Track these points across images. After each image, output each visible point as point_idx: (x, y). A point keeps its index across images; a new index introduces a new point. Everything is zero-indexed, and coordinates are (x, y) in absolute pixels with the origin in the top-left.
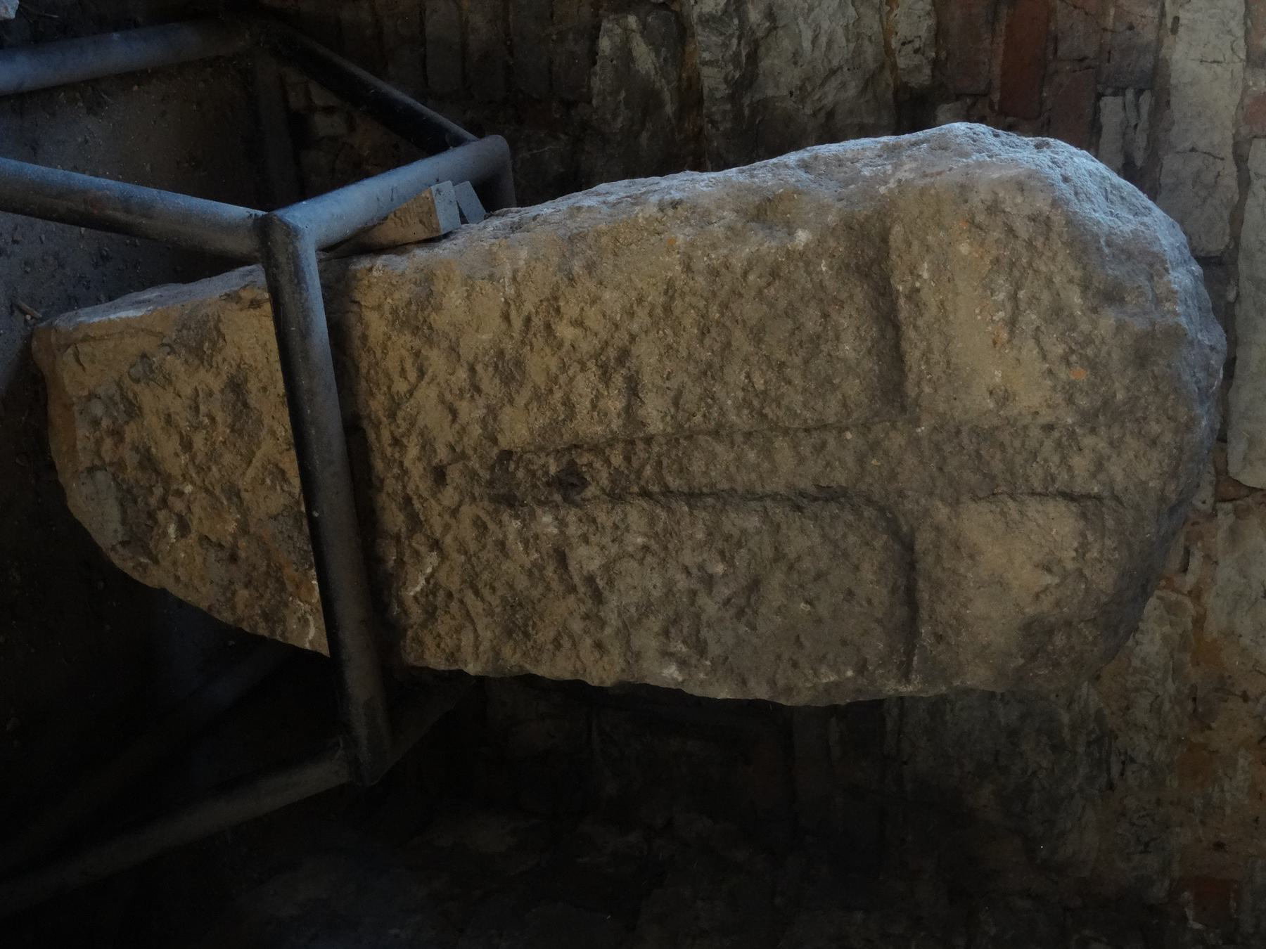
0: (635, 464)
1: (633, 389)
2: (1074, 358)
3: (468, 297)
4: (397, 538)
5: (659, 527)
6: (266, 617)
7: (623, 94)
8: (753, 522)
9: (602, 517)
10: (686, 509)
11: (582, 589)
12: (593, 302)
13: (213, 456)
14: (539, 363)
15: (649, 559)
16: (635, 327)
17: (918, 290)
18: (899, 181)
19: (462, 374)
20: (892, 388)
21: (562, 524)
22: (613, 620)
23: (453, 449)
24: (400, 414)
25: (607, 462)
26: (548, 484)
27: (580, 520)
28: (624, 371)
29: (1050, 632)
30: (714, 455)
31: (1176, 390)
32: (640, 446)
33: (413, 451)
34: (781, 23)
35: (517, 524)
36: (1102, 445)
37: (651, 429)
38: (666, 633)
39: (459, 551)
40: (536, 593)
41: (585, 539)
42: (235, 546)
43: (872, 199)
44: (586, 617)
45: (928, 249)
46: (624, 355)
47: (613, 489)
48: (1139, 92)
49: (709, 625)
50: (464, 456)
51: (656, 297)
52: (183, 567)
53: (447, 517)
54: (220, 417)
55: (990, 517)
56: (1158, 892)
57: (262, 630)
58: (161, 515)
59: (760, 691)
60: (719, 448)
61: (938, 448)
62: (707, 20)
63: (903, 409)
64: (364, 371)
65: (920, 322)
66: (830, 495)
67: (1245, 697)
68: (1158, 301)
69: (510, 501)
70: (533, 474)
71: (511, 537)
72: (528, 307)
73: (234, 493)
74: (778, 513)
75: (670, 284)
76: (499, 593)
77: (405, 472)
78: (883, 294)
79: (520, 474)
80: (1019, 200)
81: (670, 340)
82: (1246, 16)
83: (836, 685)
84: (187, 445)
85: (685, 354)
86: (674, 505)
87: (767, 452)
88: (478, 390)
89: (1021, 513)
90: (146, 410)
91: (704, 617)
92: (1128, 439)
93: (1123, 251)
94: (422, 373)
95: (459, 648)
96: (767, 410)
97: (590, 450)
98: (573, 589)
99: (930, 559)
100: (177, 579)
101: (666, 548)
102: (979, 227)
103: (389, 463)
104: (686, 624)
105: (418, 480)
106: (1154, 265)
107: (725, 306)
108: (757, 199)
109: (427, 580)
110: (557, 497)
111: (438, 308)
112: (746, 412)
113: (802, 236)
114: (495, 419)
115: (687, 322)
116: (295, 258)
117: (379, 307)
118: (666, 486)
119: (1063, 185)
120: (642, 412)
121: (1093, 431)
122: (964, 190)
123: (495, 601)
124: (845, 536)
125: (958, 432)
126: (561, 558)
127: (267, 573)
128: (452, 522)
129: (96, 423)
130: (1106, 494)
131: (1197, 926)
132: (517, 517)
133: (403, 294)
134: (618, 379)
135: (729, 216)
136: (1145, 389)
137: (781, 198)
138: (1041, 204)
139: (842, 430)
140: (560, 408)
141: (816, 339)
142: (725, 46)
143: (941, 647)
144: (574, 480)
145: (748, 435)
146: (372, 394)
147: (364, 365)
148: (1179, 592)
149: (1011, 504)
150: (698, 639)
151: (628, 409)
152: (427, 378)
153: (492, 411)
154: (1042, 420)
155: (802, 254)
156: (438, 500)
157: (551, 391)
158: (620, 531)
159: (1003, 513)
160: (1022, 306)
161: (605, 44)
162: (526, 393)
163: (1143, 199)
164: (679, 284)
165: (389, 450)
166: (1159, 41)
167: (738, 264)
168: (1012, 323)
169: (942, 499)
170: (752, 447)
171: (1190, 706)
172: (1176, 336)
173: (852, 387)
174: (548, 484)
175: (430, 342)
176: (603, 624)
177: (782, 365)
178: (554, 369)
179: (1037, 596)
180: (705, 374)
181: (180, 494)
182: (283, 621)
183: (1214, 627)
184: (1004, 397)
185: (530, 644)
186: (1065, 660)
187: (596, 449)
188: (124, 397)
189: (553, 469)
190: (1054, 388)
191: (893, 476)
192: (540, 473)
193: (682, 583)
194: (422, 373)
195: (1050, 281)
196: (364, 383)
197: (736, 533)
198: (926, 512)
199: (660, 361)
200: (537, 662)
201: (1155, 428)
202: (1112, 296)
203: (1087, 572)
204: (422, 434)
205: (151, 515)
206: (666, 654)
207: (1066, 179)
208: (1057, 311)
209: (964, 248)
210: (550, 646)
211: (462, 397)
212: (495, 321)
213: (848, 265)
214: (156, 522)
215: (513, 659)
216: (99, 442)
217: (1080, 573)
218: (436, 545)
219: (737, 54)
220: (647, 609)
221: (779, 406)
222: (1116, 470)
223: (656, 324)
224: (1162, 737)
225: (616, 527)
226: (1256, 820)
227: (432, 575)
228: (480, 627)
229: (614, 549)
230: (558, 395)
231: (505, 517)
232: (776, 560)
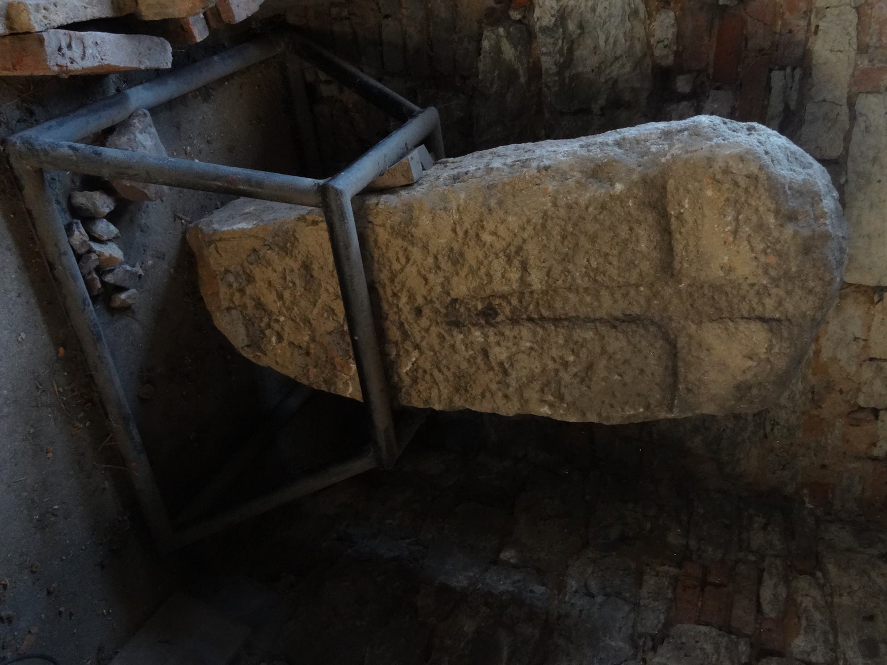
0: (525, 304)
1: (525, 267)
2: (769, 251)
3: (433, 220)
4: (396, 343)
5: (539, 338)
6: (325, 381)
7: (496, 73)
8: (589, 335)
9: (507, 332)
10: (553, 327)
11: (497, 369)
12: (502, 223)
13: (294, 303)
14: (473, 255)
15: (533, 353)
16: (526, 236)
17: (682, 213)
18: (673, 155)
19: (430, 260)
20: (667, 267)
21: (486, 336)
22: (514, 384)
23: (425, 298)
24: (396, 280)
25: (509, 303)
27: (496, 334)
28: (519, 258)
29: (750, 388)
31: (824, 265)
33: (404, 299)
34: (587, 30)
35: (461, 336)
36: (782, 293)
37: (534, 288)
38: (542, 391)
39: (430, 350)
41: (498, 344)
42: (308, 347)
43: (657, 165)
44: (499, 383)
45: (688, 192)
46: (519, 250)
47: (512, 317)
48: (794, 69)
49: (565, 386)
50: (431, 302)
51: (537, 220)
52: (280, 357)
53: (423, 333)
54: (298, 282)
55: (719, 331)
56: (790, 489)
57: (324, 388)
58: (268, 332)
59: (592, 418)
60: (571, 296)
61: (691, 295)
62: (545, 30)
63: (672, 275)
64: (376, 258)
65: (683, 230)
66: (630, 319)
67: (841, 392)
68: (816, 218)
69: (456, 324)
70: (469, 310)
71: (458, 343)
72: (467, 225)
73: (307, 321)
74: (603, 329)
75: (545, 213)
76: (452, 370)
77: (400, 310)
78: (664, 215)
79: (462, 310)
80: (741, 166)
82: (858, 24)
83: (634, 415)
84: (281, 297)
85: (553, 249)
86: (546, 325)
87: (597, 296)
88: (439, 268)
89: (736, 328)
90: (257, 278)
91: (563, 383)
92: (797, 289)
93: (798, 192)
95: (430, 397)
96: (598, 278)
97: (500, 297)
98: (492, 369)
99: (685, 351)
100: (277, 363)
102: (718, 181)
103: (391, 305)
106: (815, 197)
107: (575, 225)
109: (413, 364)
110: (483, 322)
111: (416, 226)
112: (586, 279)
114: (449, 282)
115: (555, 233)
116: (341, 207)
118: (541, 315)
119: (765, 157)
120: (529, 279)
121: (777, 286)
122: (710, 161)
123: (449, 374)
125: (702, 287)
126: (485, 353)
127: (327, 361)
128: (426, 335)
129: (230, 285)
130: (783, 318)
131: (811, 506)
132: (461, 333)
133: (397, 219)
134: (516, 263)
135: (578, 175)
136: (807, 266)
137: (606, 164)
138: (754, 169)
140: (485, 278)
141: (626, 242)
142: (555, 44)
143: (690, 395)
144: (490, 312)
145: (586, 289)
146: (381, 271)
147: (376, 256)
149: (731, 324)
151: (522, 278)
152: (411, 262)
153: (447, 279)
154: (748, 281)
155: (618, 197)
157: (479, 269)
158: (517, 340)
159: (726, 329)
160: (741, 223)
161: (486, 44)
164: (549, 213)
165: (390, 299)
166: (807, 39)
167: (583, 202)
168: (735, 233)
169: (692, 322)
170: (588, 295)
171: (810, 396)
172: (826, 237)
173: (645, 266)
174: (477, 315)
175: (413, 244)
176: (508, 386)
177: (607, 254)
178: (481, 257)
179: (744, 372)
180: (564, 260)
181: (277, 321)
182: (335, 384)
183: (825, 356)
184: (730, 270)
185: (468, 395)
186: (756, 400)
187: (503, 297)
188: (244, 272)
189: (480, 307)
190: (757, 266)
191: (666, 309)
192: (472, 309)
193: (551, 365)
196: (376, 265)
197: (581, 340)
198: (684, 328)
199: (539, 253)
200: (473, 405)
201: (811, 284)
202: (792, 217)
203: (772, 359)
204: (409, 291)
205: (262, 332)
206: (543, 401)
207: (766, 153)
208: (761, 226)
211: (430, 272)
212: (449, 233)
213: (644, 203)
214: (264, 334)
215: (459, 403)
216: (232, 295)
217: (768, 360)
218: (417, 347)
219: (562, 49)
220: (531, 379)
221: (604, 275)
222: (789, 306)
223: (537, 234)
224: (794, 412)
225: (515, 337)
226: (845, 453)
227: (415, 362)
229: (514, 349)
230: (483, 270)
231: (455, 333)
232: (602, 354)
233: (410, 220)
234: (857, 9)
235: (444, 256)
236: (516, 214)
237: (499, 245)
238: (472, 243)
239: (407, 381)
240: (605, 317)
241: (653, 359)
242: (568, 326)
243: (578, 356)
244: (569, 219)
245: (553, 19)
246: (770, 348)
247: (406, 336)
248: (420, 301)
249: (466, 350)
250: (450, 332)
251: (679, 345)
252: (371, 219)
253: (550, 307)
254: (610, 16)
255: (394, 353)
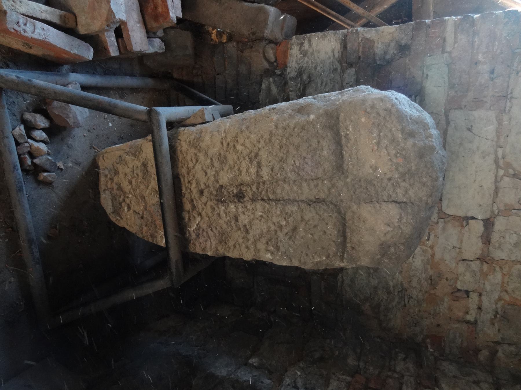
1: (259, 165)
2: (398, 155)
4: (189, 212)
5: (266, 210)
6: (151, 236)
7: (268, 100)
8: (295, 208)
11: (242, 229)
12: (248, 138)
13: (138, 186)
14: (231, 157)
15: (263, 219)
16: (260, 146)
17: (348, 135)
18: (343, 100)
19: (209, 161)
20: (340, 167)
21: (237, 208)
22: (252, 239)
24: (191, 174)
25: (251, 189)
26: (233, 196)
28: (257, 160)
29: (389, 247)
30: (284, 188)
31: (432, 167)
32: (261, 184)
33: (194, 185)
34: (312, 79)
35: (223, 208)
36: (407, 186)
37: (264, 179)
38: (267, 243)
40: (229, 230)
42: (143, 213)
43: (334, 105)
44: (243, 238)
45: (352, 121)
46: (257, 155)
47: (253, 198)
48: (416, 96)
50: (209, 187)
52: (129, 221)
53: (203, 205)
54: (140, 174)
55: (370, 208)
56: (420, 338)
57: (150, 240)
58: (123, 204)
59: (296, 264)
60: (286, 186)
61: (354, 186)
62: (292, 79)
63: (343, 173)
64: (180, 160)
65: (349, 145)
66: (318, 201)
67: (447, 279)
68: (427, 138)
71: (222, 212)
73: (143, 198)
74: (303, 205)
75: (271, 132)
76: (218, 230)
77: (191, 191)
78: (337, 134)
81: (271, 150)
82: (448, 73)
83: (320, 262)
84: (130, 183)
85: (275, 154)
86: (271, 203)
87: (300, 187)
88: (214, 166)
89: (380, 207)
90: (120, 172)
91: (279, 239)
92: (416, 183)
93: (415, 121)
94: (197, 161)
95: (206, 247)
96: (300, 173)
98: (240, 229)
99: (350, 222)
100: (127, 224)
101: (268, 216)
102: (368, 113)
103: (187, 188)
104: (274, 240)
105: (195, 194)
106: (425, 126)
107: (287, 139)
108: (299, 107)
109: (197, 225)
110: (236, 200)
111: (202, 141)
112: (293, 173)
113: (312, 117)
114: (218, 175)
115: (276, 144)
116: (158, 121)
117: (185, 141)
120: (261, 173)
121: (404, 181)
122: (364, 101)
124: (323, 213)
125: (360, 181)
127: (152, 222)
128: (204, 207)
129: (106, 176)
130: (408, 201)
131: (431, 350)
132: (223, 206)
133: (193, 137)
134: (255, 163)
135: (290, 111)
136: (422, 166)
138: (389, 106)
139: (323, 180)
140: (237, 171)
141: (315, 150)
142: (296, 86)
143: (354, 251)
144: (241, 195)
145: (294, 181)
146: (182, 167)
147: (180, 158)
148: (426, 246)
149: (377, 204)
150: (277, 246)
151: (257, 172)
152: (198, 162)
153: (217, 173)
154: (387, 176)
155: (312, 122)
156: (201, 200)
157: (235, 166)
158: (254, 210)
159: (374, 207)
160: (382, 138)
161: (263, 86)
162: (227, 166)
163: (420, 108)
164: (273, 132)
165: (187, 185)
166: (422, 82)
168: (378, 143)
169: (354, 202)
170: (295, 185)
171: (430, 281)
172: (432, 149)
173: (327, 165)
174: (233, 196)
175: (200, 151)
176: (248, 240)
177: (305, 158)
178: (236, 159)
180: (281, 161)
181: (128, 197)
182: (156, 237)
183: (437, 257)
185: (227, 246)
186: (393, 257)
187: (248, 185)
188: (114, 168)
189: (235, 192)
190: (392, 165)
192: (231, 193)
193: (273, 228)
194: (197, 161)
195: (391, 130)
196: (180, 164)
197: (290, 212)
198: (350, 207)
200: (229, 252)
201: (425, 179)
202: (411, 135)
203: (402, 227)
204: (196, 180)
205: (120, 204)
206: (267, 250)
207: (396, 99)
208: (393, 140)
209: (363, 120)
210: (233, 247)
211: (208, 168)
212: (219, 144)
213: (326, 126)
214: (122, 206)
215: (222, 251)
216: (107, 182)
217: (400, 228)
218: (200, 214)
219: (300, 88)
220: (261, 236)
221: (304, 171)
222: (411, 193)
223: (266, 145)
224: (421, 291)
225: (253, 209)
226: (450, 318)
227: (198, 224)
228: (212, 240)
229: (252, 216)
230: (237, 167)
231: (220, 206)
232: (302, 221)
233: (199, 139)
237: (245, 152)
238: (231, 151)
239: (194, 236)
240: (304, 199)
242: (283, 204)
246: (400, 219)
247: (194, 207)
250: (217, 205)
251: (347, 218)
252: (180, 138)
253: (274, 192)
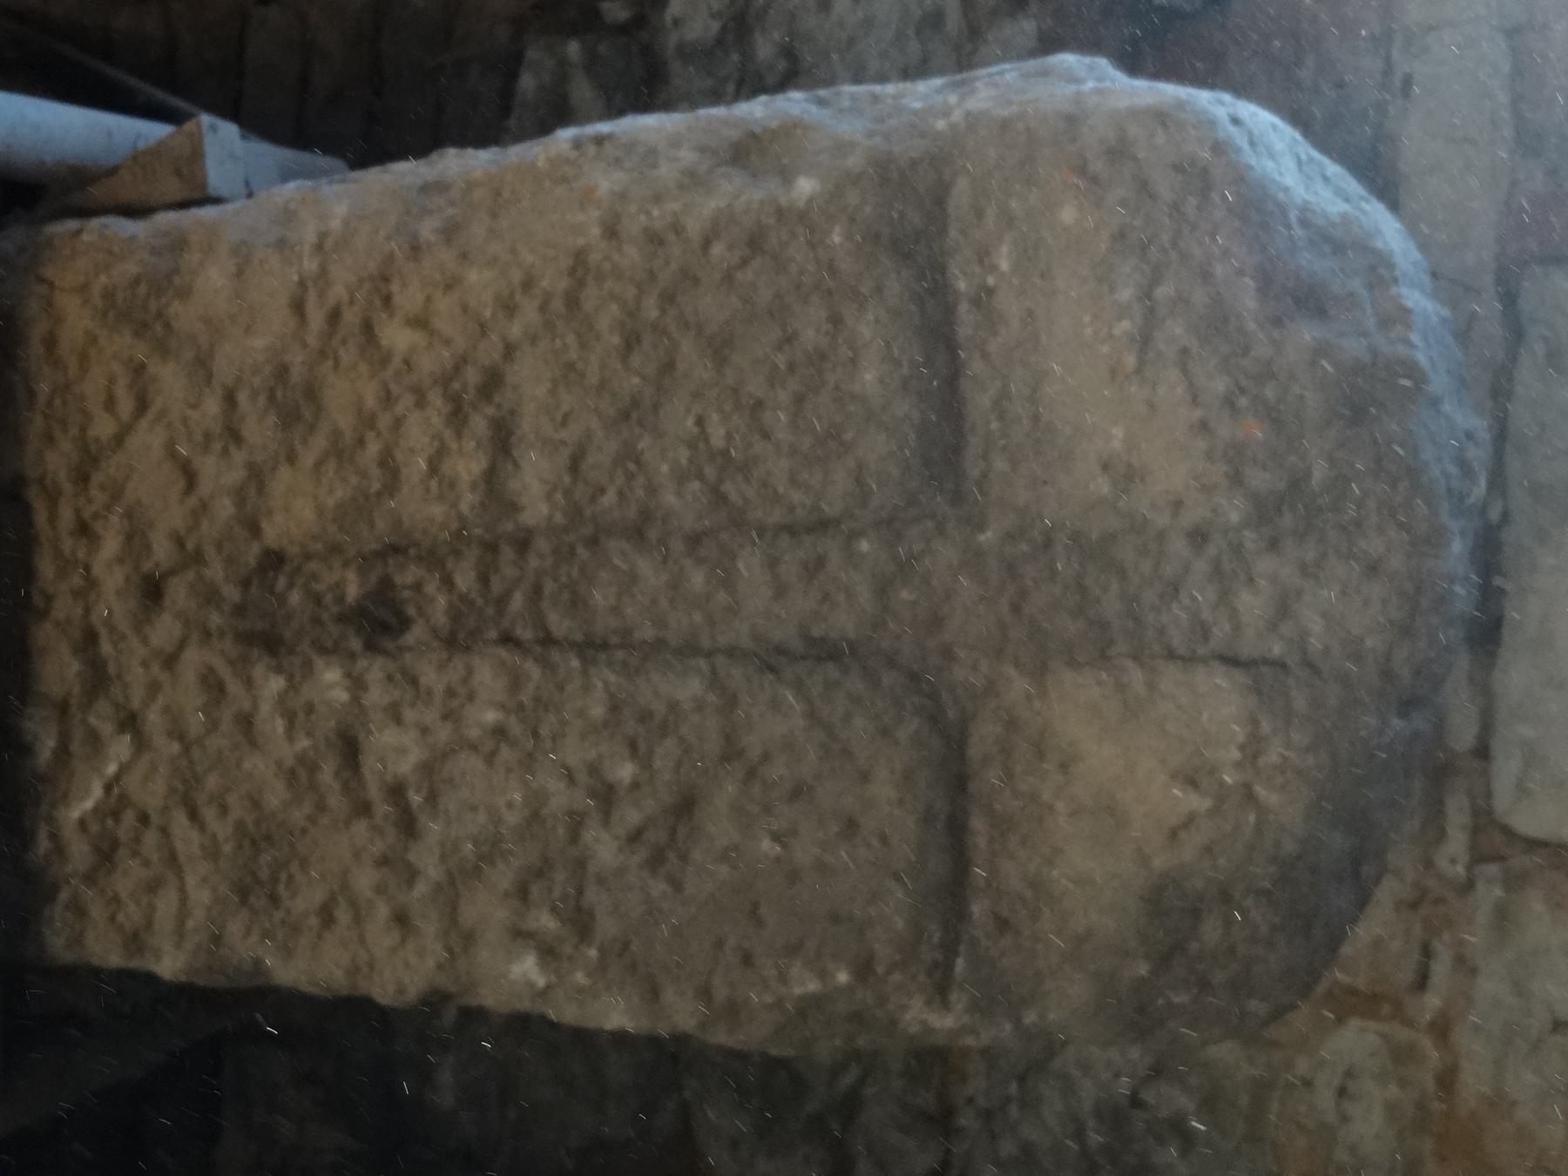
0: (496, 587)
1: (503, 440)
2: (1243, 402)
3: (240, 273)
4: (63, 708)
5: (525, 697)
9: (429, 676)
10: (575, 663)
12: (448, 287)
14: (346, 392)
15: (505, 753)
16: (515, 331)
17: (990, 292)
18: (968, 114)
19: (212, 406)
21: (357, 685)
22: (432, 870)
23: (179, 542)
24: (97, 478)
25: (448, 582)
26: (341, 619)
27: (390, 678)
28: (490, 411)
29: (1195, 914)
30: (633, 578)
32: (507, 553)
33: (111, 545)
35: (276, 684)
38: (522, 893)
39: (170, 734)
40: (298, 816)
41: (395, 714)
44: (383, 862)
46: (493, 381)
47: (453, 633)
49: (601, 881)
51: (554, 281)
53: (156, 669)
59: (682, 1014)
60: (645, 567)
61: (1011, 569)
62: (687, 53)
63: (958, 498)
64: (41, 399)
65: (993, 346)
66: (825, 651)
68: (1385, 323)
69: (267, 641)
70: (317, 600)
71: (265, 708)
72: (338, 292)
74: (735, 675)
75: (580, 257)
77: (91, 583)
79: (295, 598)
80: (1160, 139)
81: (573, 355)
85: (593, 379)
88: (234, 435)
91: (592, 868)
94: (142, 405)
95: (149, 924)
96: (727, 487)
97: (420, 559)
98: (363, 809)
101: (536, 734)
104: (560, 876)
105: (113, 598)
106: (1379, 270)
107: (668, 298)
108: (734, 134)
109: (108, 788)
110: (355, 644)
111: (185, 293)
113: (806, 186)
114: (261, 490)
115: (603, 323)
117: (83, 289)
118: (546, 629)
119: (1232, 129)
120: (513, 485)
121: (1274, 545)
122: (1073, 121)
123: (222, 830)
124: (847, 717)
125: (1048, 543)
126: (350, 749)
128: (164, 677)
132: (279, 670)
134: (479, 423)
137: (774, 135)
139: (853, 536)
140: (375, 472)
145: (695, 540)
146: (50, 439)
147: (44, 388)
148: (1408, 1022)
150: (579, 908)
151: (491, 478)
152: (151, 413)
153: (257, 476)
154: (1189, 518)
155: (803, 216)
156: (145, 641)
157: (361, 442)
159: (1121, 687)
161: (527, 83)
162: (320, 442)
163: (1353, 186)
164: (594, 258)
165: (67, 544)
167: (694, 227)
168: (1144, 341)
169: (1017, 665)
170: (700, 561)
173: (875, 447)
174: (341, 619)
175: (163, 350)
176: (411, 875)
177: (759, 404)
178: (371, 402)
179: (1173, 835)
183: (1474, 1083)
184: (1128, 476)
185: (278, 915)
186: (1219, 977)
187: (433, 559)
189: (353, 591)
190: (1209, 456)
191: (936, 622)
192: (329, 598)
194: (142, 405)
195: (1206, 275)
197: (659, 708)
199: (553, 392)
200: (287, 952)
201: (1372, 545)
203: (1260, 791)
204: (129, 515)
206: (520, 935)
207: (1236, 121)
209: (1068, 215)
210: (314, 921)
213: (877, 237)
217: (1249, 796)
218: (130, 722)
220: (491, 849)
225: (450, 692)
227: (117, 778)
228: (191, 881)
229: (443, 734)
230: (373, 448)
231: (258, 671)
233: (167, 277)
234: (1513, 33)
235: (254, 395)
236: (493, 261)
237: (429, 364)
238: (347, 355)
239: (80, 852)
240: (746, 643)
241: (889, 799)
242: (625, 664)
243: (646, 763)
244: (652, 275)
245: (715, 26)
246: (1253, 748)
247: (98, 678)
248: (162, 551)
249: (290, 735)
250: (241, 666)
251: (975, 751)
252: (48, 272)
253: (577, 603)
254: (869, 23)
255: (46, 746)
